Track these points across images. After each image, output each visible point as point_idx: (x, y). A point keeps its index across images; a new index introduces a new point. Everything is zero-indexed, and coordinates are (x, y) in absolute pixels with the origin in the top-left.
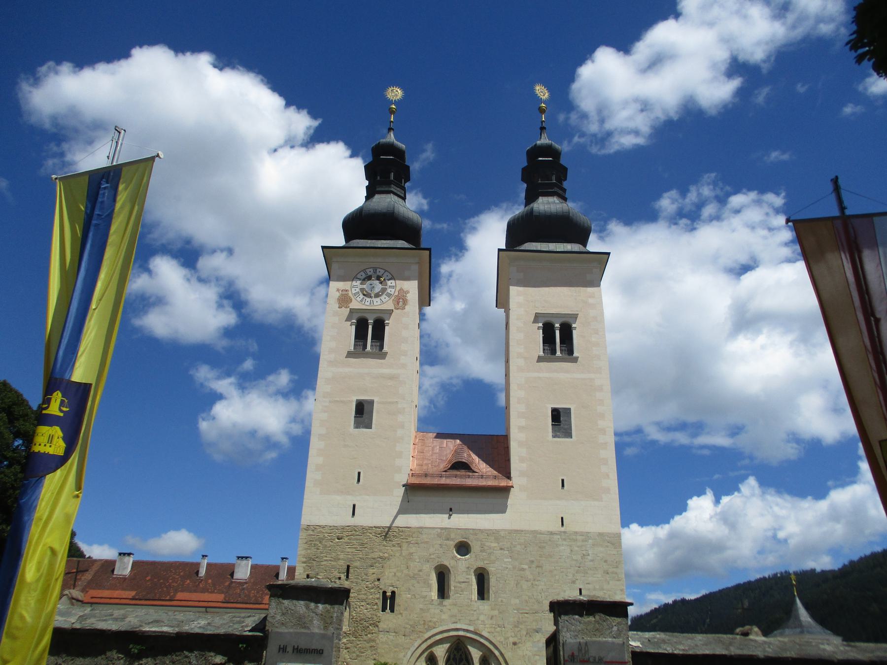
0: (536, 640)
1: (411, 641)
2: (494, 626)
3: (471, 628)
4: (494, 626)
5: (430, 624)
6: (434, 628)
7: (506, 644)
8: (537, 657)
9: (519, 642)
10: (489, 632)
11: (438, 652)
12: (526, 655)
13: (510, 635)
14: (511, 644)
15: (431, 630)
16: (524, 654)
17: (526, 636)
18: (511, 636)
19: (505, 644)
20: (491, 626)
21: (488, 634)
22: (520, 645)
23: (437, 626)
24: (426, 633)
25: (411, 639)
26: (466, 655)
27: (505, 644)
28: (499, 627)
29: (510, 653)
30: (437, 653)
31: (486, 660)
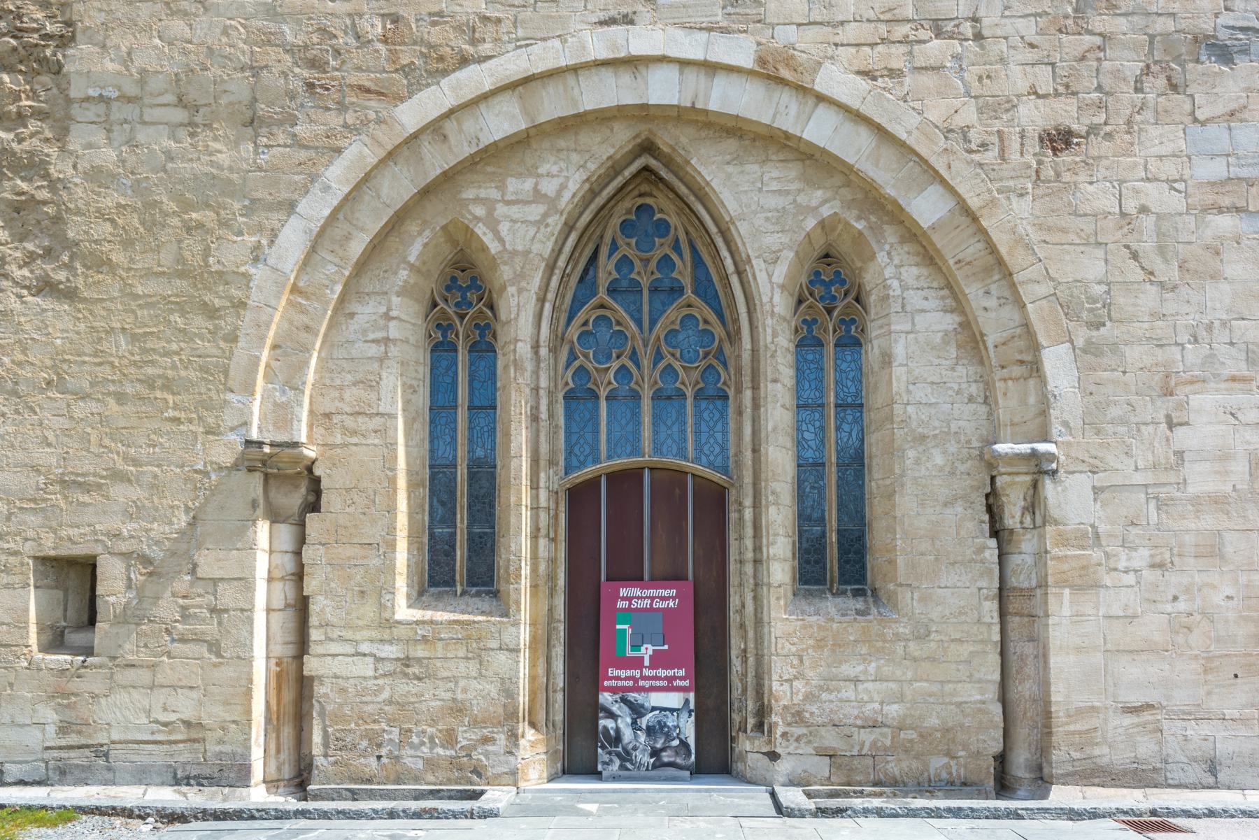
0: (1220, 109)
1: (303, 155)
2: (901, 31)
3: (740, 52)
4: (901, 31)
5: (436, 35)
6: (464, 61)
7: (995, 139)
8: (1225, 223)
9: (1093, 130)
10: (866, 74)
11: (504, 228)
12: (1144, 209)
13: (1022, 85)
14: (1033, 146)
15: (445, 73)
16: (1131, 206)
17: (1137, 90)
18: (1035, 93)
19: (984, 146)
20: (883, 29)
21: (863, 84)
22: (1097, 146)
23: (485, 49)
24: (402, 99)
25: (297, 143)
26: (698, 262)
27: (984, 146)
28: (939, 34)
29: (1022, 208)
30: (492, 223)
31: (839, 279)
